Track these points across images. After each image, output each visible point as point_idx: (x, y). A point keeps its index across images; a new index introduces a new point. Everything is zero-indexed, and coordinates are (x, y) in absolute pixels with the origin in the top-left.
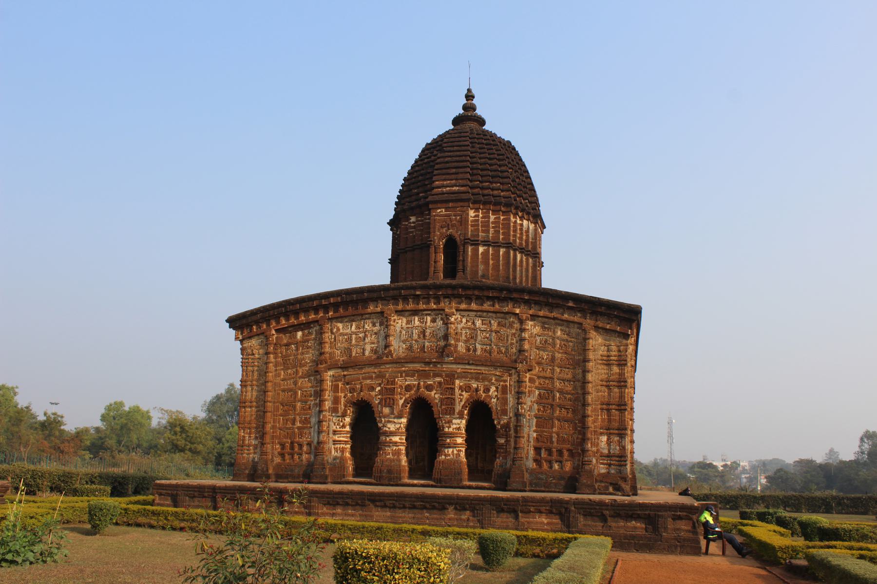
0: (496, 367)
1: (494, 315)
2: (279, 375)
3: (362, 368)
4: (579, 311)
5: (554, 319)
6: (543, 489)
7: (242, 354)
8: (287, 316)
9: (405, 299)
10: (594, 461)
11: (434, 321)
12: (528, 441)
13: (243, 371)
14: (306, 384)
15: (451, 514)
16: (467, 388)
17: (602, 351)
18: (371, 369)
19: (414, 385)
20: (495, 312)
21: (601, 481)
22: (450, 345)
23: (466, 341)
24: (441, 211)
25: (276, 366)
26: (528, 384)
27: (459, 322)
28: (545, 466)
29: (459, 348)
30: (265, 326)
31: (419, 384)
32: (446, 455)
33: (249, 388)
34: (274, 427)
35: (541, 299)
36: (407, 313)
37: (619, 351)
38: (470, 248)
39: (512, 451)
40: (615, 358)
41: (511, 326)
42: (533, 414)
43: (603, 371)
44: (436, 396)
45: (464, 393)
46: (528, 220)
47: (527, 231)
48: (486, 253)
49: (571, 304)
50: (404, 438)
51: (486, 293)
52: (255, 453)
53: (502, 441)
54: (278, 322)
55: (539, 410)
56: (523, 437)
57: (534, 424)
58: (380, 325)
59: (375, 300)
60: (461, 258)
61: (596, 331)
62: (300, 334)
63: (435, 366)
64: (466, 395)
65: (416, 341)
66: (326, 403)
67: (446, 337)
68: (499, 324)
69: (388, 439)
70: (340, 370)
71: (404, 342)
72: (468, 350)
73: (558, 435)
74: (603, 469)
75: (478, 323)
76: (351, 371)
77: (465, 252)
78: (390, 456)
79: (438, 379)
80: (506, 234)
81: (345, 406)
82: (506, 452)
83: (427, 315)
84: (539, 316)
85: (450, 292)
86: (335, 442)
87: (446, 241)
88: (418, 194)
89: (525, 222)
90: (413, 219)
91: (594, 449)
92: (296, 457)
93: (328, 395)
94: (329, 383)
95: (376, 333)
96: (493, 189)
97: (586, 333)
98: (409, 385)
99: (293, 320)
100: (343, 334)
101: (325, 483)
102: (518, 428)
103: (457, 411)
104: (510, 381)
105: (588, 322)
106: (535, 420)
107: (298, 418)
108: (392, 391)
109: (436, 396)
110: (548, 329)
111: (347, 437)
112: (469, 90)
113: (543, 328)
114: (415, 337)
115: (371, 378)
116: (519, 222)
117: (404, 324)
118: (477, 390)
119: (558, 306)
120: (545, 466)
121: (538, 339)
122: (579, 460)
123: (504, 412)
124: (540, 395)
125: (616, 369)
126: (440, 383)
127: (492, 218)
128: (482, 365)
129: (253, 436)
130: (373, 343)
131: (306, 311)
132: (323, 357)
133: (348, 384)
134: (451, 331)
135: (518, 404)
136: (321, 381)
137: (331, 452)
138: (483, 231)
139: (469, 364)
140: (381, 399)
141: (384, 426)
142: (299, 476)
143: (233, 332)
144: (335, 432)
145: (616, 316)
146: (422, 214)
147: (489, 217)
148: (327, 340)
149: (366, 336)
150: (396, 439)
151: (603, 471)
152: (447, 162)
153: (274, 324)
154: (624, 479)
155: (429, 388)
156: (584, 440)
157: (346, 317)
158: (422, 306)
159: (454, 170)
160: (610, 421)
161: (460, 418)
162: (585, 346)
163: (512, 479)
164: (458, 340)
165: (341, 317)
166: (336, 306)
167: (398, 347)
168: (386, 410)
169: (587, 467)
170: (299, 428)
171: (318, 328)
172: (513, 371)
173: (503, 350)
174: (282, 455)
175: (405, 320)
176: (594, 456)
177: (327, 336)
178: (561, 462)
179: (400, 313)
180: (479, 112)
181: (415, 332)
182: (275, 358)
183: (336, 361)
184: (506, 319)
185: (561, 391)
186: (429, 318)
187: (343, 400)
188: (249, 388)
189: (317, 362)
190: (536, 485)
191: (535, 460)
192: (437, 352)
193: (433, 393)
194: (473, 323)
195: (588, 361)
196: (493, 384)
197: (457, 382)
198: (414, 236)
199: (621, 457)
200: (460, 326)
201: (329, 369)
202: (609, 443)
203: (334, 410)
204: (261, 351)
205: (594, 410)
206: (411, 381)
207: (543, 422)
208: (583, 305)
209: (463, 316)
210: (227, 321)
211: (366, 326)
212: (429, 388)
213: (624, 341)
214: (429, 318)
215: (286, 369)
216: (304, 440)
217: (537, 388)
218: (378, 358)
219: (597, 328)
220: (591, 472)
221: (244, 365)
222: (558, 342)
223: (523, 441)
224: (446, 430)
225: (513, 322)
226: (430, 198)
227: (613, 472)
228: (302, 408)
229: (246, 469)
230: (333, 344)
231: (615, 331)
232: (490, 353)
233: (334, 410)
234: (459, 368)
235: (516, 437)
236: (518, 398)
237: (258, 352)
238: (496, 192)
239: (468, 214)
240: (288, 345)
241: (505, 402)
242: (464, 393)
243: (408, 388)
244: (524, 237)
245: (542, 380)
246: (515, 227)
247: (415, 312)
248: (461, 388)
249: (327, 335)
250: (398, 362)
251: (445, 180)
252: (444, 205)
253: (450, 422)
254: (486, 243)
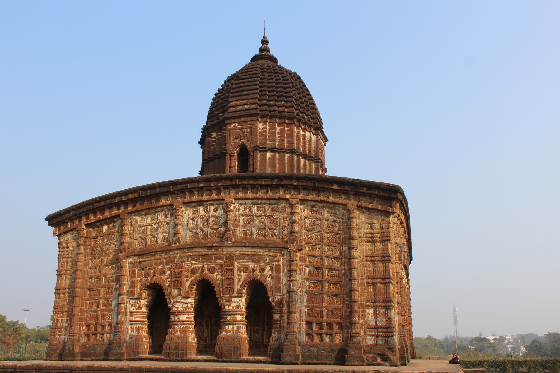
0: (269, 248)
1: (268, 202)
2: (88, 265)
3: (155, 255)
4: (343, 193)
5: (321, 201)
6: (315, 361)
7: (59, 248)
8: (95, 215)
10: (362, 333)
11: (216, 210)
12: (300, 316)
13: (59, 262)
14: (110, 271)
16: (245, 269)
17: (366, 229)
19: (199, 269)
21: (369, 353)
22: (229, 230)
23: (243, 227)
24: (235, 125)
25: (85, 256)
26: (299, 262)
27: (238, 210)
28: (317, 339)
29: (238, 233)
30: (77, 223)
31: (203, 267)
32: (226, 332)
33: (64, 277)
34: (81, 310)
35: (308, 184)
36: (193, 205)
37: (382, 228)
38: (259, 155)
39: (285, 325)
40: (379, 235)
41: (283, 211)
42: (304, 290)
43: (368, 248)
44: (218, 277)
45: (242, 274)
46: (310, 132)
47: (310, 140)
48: (273, 159)
49: (335, 187)
50: (192, 317)
51: (259, 182)
52: (66, 335)
54: (88, 219)
55: (309, 286)
56: (295, 312)
57: (306, 299)
58: (171, 216)
59: (166, 194)
60: (251, 163)
61: (359, 210)
62: (105, 228)
63: (217, 250)
64: (243, 275)
65: (201, 228)
66: (125, 287)
67: (226, 224)
68: (273, 210)
69: (176, 318)
70: (137, 258)
71: (191, 230)
72: (246, 234)
73: (327, 309)
74: (370, 341)
76: (146, 258)
77: (254, 158)
78: (178, 334)
79: (219, 262)
80: (291, 142)
81: (141, 289)
82: (280, 327)
83: (210, 205)
84: (307, 200)
85: (228, 183)
86: (132, 322)
87: (240, 150)
88: (218, 114)
89: (308, 134)
90: (214, 135)
91: (362, 321)
92: (99, 336)
93: (126, 280)
94: (128, 270)
95: (167, 224)
97: (350, 213)
98: (194, 268)
99: (100, 216)
100: (140, 226)
101: (120, 360)
102: (290, 303)
103: (236, 290)
104: (282, 260)
105: (352, 203)
106: (306, 296)
107: (101, 301)
108: (180, 274)
109: (218, 277)
110: (316, 211)
111: (143, 318)
112: (264, 37)
113: (312, 211)
114: (200, 224)
115: (162, 263)
116: (301, 132)
117: (191, 215)
118: (253, 270)
119: (324, 190)
120: (317, 339)
121: (308, 221)
122: (348, 333)
123: (278, 290)
124: (310, 272)
125: (379, 245)
126: (221, 265)
127: (278, 129)
128: (257, 247)
129: (65, 319)
130: (165, 232)
131: (110, 207)
132: (122, 247)
133: (143, 269)
134: (230, 218)
135: (290, 281)
136: (120, 268)
137: (127, 331)
138: (270, 140)
139: (245, 247)
140: (171, 282)
141: (173, 306)
142: (100, 355)
143: (51, 229)
144: (132, 313)
145: (377, 196)
146: (220, 130)
147: (275, 129)
148: (127, 232)
149: (159, 226)
150: (184, 318)
151: (371, 343)
152: (241, 87)
153: (85, 220)
154: (392, 350)
155: (212, 270)
156: (351, 313)
157: (142, 210)
158: (205, 197)
159: (246, 93)
160: (375, 294)
161: (238, 297)
162: (349, 225)
163: (285, 353)
164: (236, 226)
165: (139, 211)
167: (185, 235)
168: (175, 292)
169: (355, 339)
170: (102, 311)
171: (120, 221)
172: (285, 251)
173: (276, 232)
174: (87, 335)
175: (191, 210)
176: (362, 328)
177: (127, 229)
178: (331, 335)
179: (187, 204)
180: (272, 53)
181: (200, 220)
182: (85, 249)
183: (134, 249)
184: (278, 204)
185: (329, 268)
186: (212, 208)
187: (139, 284)
188: (64, 277)
189: (118, 251)
190: (309, 357)
191: (307, 334)
192: (219, 237)
193: (215, 274)
194: (250, 210)
195: (353, 239)
196: (267, 264)
197: (236, 263)
198: (215, 148)
199: (387, 328)
200: (238, 213)
201: (128, 257)
202: (376, 315)
204: (75, 244)
205: (360, 284)
206: (197, 265)
207: (313, 297)
208: (346, 188)
209: (241, 204)
210: (46, 219)
211: (159, 218)
212: (212, 270)
213: (386, 219)
214: (212, 208)
215: (93, 259)
216: (106, 321)
217: (307, 266)
218: (169, 245)
219: (360, 208)
220: (358, 343)
221: (60, 257)
222: (326, 223)
223: (296, 316)
224: (227, 308)
225: (285, 207)
226: (226, 115)
227: (380, 342)
228: (106, 293)
229: (58, 349)
230: (132, 236)
231: (377, 210)
232: (265, 236)
233: (131, 293)
234: (237, 251)
235: (288, 312)
236: (290, 276)
237: (72, 245)
238: (281, 109)
239: (257, 127)
240: (95, 238)
241: (278, 280)
242: (242, 274)
243: (194, 271)
244: (307, 146)
245: (312, 259)
246: (298, 136)
247: (200, 203)
248: (239, 269)
249: (126, 227)
250: (184, 248)
251: (238, 100)
252: (237, 120)
253: (230, 301)
254: (273, 150)
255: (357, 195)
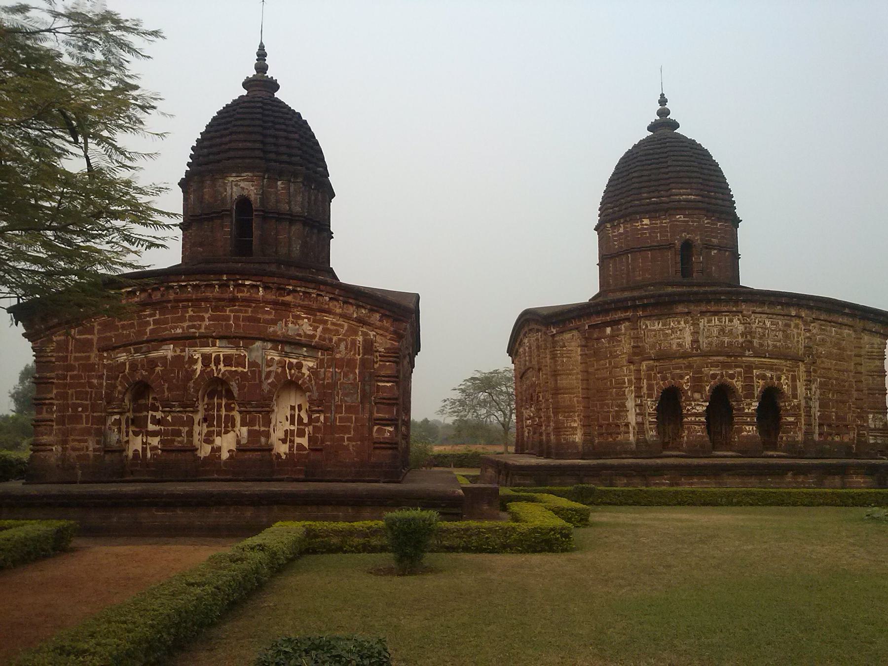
0: (786, 359)
9: (708, 302)
15: (789, 477)
16: (764, 377)
18: (680, 360)
20: (783, 315)
23: (760, 338)
49: (847, 311)
53: (791, 419)
55: (821, 394)
62: (609, 330)
72: (761, 345)
75: (768, 324)
79: (739, 369)
93: (645, 383)
96: (716, 199)
108: (700, 380)
112: (662, 95)
115: (681, 368)
118: (772, 378)
123: (795, 396)
126: (740, 373)
136: (638, 371)
151: (872, 442)
152: (679, 171)
155: (732, 377)
159: (688, 180)
166: (644, 307)
167: (704, 342)
168: (697, 396)
203: (650, 396)
212: (732, 377)
224: (746, 411)
227: (879, 442)
228: (617, 394)
240: (598, 339)
241: (794, 388)
243: (714, 376)
247: (715, 313)
248: (757, 376)
251: (682, 188)
255: (863, 318)
